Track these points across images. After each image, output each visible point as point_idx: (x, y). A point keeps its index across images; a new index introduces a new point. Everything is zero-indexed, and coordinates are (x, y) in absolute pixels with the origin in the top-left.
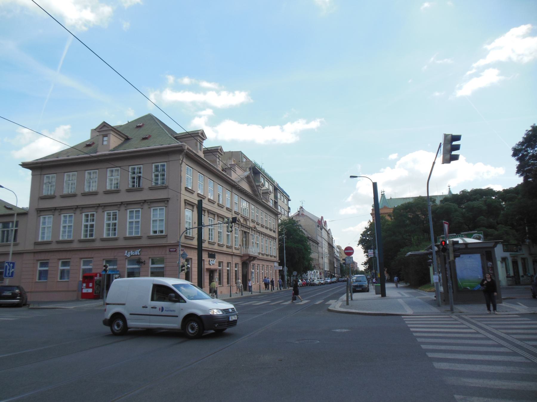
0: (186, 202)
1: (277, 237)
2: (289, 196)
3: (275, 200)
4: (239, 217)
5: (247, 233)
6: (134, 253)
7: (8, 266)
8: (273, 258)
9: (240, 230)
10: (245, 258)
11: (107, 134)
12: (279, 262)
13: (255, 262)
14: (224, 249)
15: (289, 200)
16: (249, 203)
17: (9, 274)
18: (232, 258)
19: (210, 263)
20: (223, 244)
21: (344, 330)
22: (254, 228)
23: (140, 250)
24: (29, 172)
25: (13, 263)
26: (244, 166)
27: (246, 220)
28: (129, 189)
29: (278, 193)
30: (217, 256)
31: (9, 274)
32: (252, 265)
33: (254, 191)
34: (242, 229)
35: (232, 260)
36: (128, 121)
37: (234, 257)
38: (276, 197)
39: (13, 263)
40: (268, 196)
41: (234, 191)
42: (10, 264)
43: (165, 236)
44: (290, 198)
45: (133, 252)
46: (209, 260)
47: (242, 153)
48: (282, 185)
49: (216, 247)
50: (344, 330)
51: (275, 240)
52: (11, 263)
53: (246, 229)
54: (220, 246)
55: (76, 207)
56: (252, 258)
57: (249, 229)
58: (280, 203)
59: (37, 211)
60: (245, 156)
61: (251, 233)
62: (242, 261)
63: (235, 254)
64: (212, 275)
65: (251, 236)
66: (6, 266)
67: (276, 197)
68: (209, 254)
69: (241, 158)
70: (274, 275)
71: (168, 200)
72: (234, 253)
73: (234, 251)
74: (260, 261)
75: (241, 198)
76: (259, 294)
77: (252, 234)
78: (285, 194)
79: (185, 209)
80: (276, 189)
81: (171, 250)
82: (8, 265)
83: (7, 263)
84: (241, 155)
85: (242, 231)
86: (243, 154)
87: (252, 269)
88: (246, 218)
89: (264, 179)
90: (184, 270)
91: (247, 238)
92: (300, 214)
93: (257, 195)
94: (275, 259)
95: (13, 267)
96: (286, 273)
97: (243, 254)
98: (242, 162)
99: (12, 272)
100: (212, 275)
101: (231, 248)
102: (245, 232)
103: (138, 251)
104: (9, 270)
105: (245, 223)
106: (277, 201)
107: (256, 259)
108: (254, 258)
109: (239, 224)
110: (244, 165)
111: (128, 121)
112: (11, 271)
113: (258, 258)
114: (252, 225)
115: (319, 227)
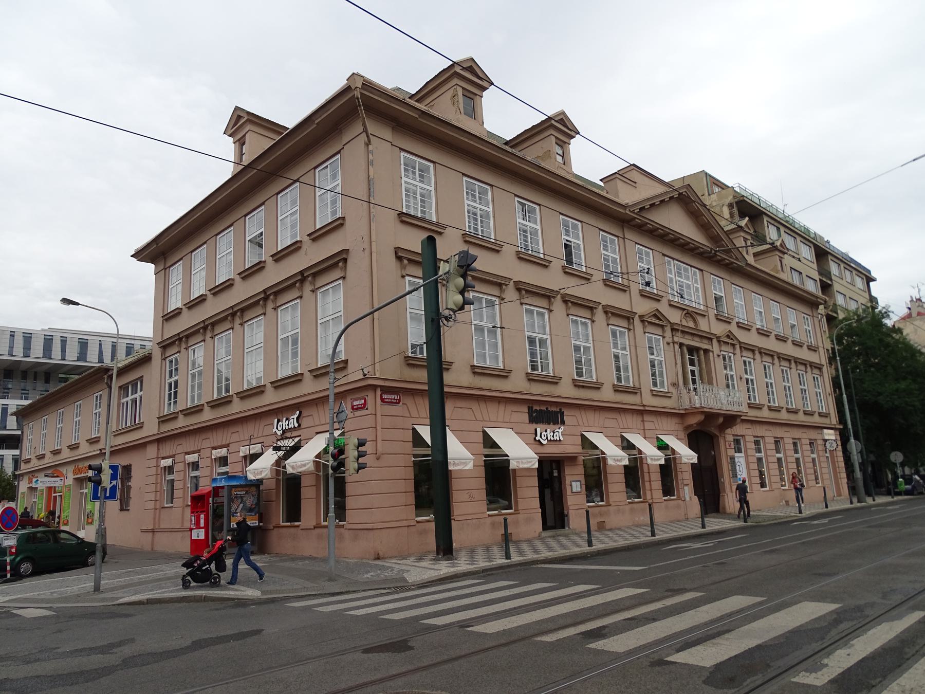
0: (400, 254)
1: (824, 362)
2: (869, 272)
3: (824, 279)
4: (664, 308)
5: (702, 352)
6: (288, 425)
8: (816, 419)
9: (668, 344)
10: (693, 420)
12: (839, 429)
13: (739, 429)
14: (607, 395)
15: (869, 279)
18: (643, 421)
19: (538, 438)
22: (728, 336)
23: (298, 412)
24: (150, 268)
26: (714, 204)
27: (690, 314)
29: (832, 264)
30: (570, 417)
32: (730, 438)
33: (715, 239)
34: (676, 339)
35: (644, 426)
37: (646, 418)
38: (824, 272)
41: (629, 235)
43: (341, 365)
44: (874, 274)
45: (287, 421)
46: (536, 430)
47: (706, 174)
48: (839, 242)
49: (565, 391)
51: (816, 371)
53: (697, 339)
54: (583, 387)
56: (721, 420)
57: (711, 340)
60: (715, 182)
62: (686, 428)
63: (647, 408)
64: (556, 474)
65: (719, 363)
67: (824, 272)
68: (530, 412)
69: (705, 186)
70: (824, 465)
71: (344, 256)
72: (644, 406)
73: (650, 401)
74: (765, 427)
75: (664, 255)
76: (740, 523)
77: (723, 353)
78: (852, 265)
79: (403, 277)
80: (822, 253)
81: (355, 403)
84: (705, 178)
85: (681, 345)
86: (710, 176)
87: (731, 452)
88: (691, 309)
89: (778, 229)
91: (704, 366)
92: (914, 315)
94: (825, 421)
96: (856, 457)
97: (686, 409)
98: (709, 195)
100: (556, 474)
101: (636, 393)
102: (692, 350)
103: (295, 417)
105: (691, 324)
106: (829, 282)
107: (738, 420)
108: (731, 419)
109: (662, 327)
110: (715, 201)
113: (742, 418)
114: (718, 329)
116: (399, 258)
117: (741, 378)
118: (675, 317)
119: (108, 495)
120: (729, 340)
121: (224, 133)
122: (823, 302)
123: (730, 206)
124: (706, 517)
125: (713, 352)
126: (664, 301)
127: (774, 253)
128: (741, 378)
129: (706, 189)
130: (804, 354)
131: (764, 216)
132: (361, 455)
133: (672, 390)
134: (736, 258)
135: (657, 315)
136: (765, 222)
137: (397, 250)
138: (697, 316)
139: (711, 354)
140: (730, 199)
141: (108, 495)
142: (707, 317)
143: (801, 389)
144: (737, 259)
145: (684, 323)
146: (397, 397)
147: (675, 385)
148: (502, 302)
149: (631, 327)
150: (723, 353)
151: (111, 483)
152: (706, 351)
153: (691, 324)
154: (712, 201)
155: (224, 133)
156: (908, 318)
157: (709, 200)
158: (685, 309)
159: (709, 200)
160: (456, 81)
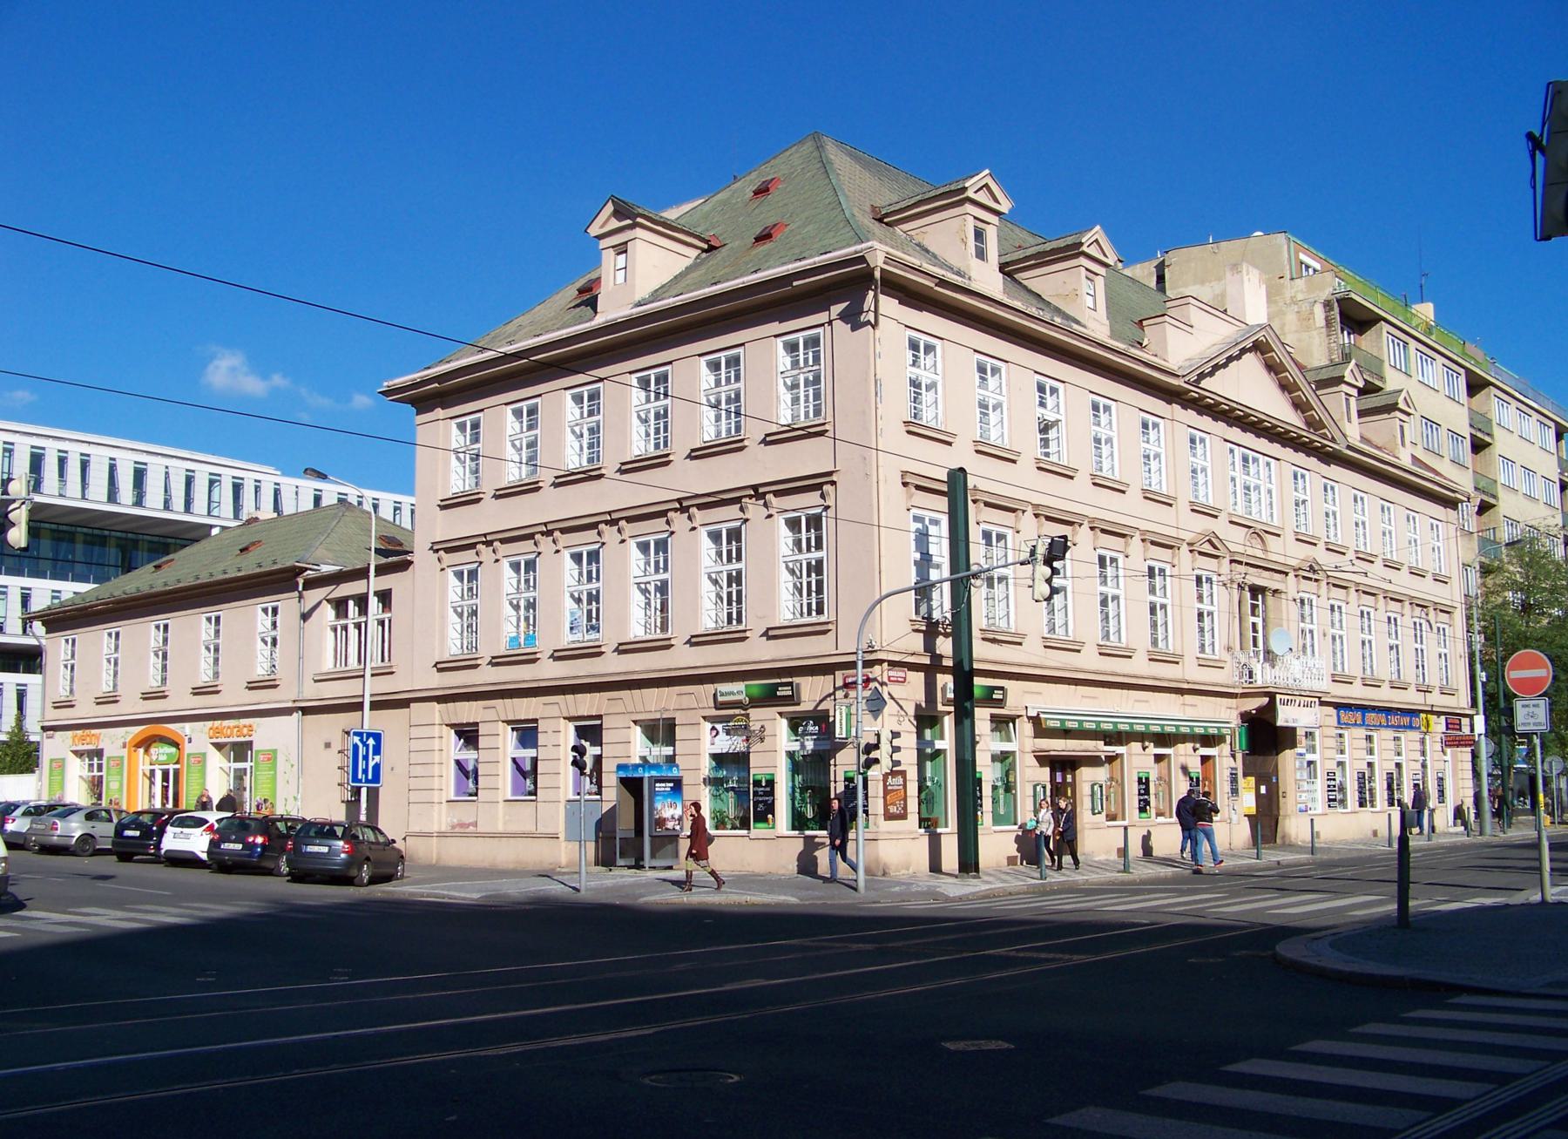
3: (1479, 435)
4: (1221, 527)
11: (626, 243)
17: (365, 771)
20: (1126, 649)
21: (993, 1045)
25: (377, 737)
27: (1260, 534)
28: (703, 445)
31: (365, 771)
39: (377, 737)
40: (1398, 422)
42: (367, 739)
50: (993, 1045)
52: (369, 735)
58: (1502, 443)
61: (1292, 593)
65: (1294, 609)
77: (1301, 594)
82: (361, 741)
83: (355, 734)
84: (1286, 247)
88: (1259, 526)
90: (877, 761)
93: (1314, 424)
95: (377, 751)
98: (1292, 279)
99: (377, 768)
102: (1256, 591)
104: (366, 758)
112: (371, 764)
114: (1296, 554)
116: (905, 484)
117: (1325, 635)
118: (1236, 539)
119: (370, 777)
120: (1311, 572)
123: (1327, 305)
124: (1264, 848)
126: (1223, 517)
127: (1393, 414)
128: (1325, 635)
129: (1288, 267)
130: (1426, 589)
131: (1383, 322)
132: (896, 749)
133: (1226, 656)
134: (1333, 437)
136: (1385, 334)
137: (904, 473)
143: (1417, 649)
144: (1333, 440)
145: (1250, 551)
146: (903, 675)
147: (1229, 649)
148: (1062, 575)
149: (1176, 562)
150: (1301, 594)
153: (1260, 554)
158: (1250, 527)
159: (1292, 288)
160: (969, 208)
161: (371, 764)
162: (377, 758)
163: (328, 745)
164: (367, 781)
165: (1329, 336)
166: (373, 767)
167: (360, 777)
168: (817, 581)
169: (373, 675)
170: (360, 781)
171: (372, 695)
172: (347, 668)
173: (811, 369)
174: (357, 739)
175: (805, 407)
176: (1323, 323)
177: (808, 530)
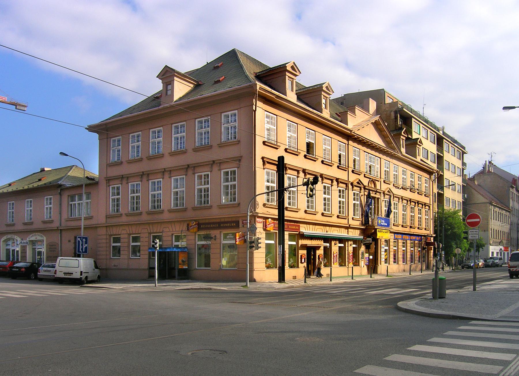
3: (439, 153)
4: (361, 178)
7: (80, 240)
11: (171, 81)
16: (380, 158)
17: (82, 249)
25: (86, 239)
31: (82, 249)
36: (207, 62)
39: (86, 239)
42: (83, 239)
52: (83, 238)
55: (142, 174)
59: (106, 180)
66: (79, 241)
82: (81, 239)
83: (79, 237)
95: (86, 243)
104: (82, 245)
106: (442, 155)
110: (388, 108)
111: (207, 62)
112: (84, 247)
115: (514, 189)
119: (84, 251)
121: (157, 77)
122: (436, 172)
125: (381, 199)
135: (359, 183)
138: (376, 181)
139: (380, 200)
140: (396, 108)
141: (84, 251)
142: (380, 182)
151: (85, 245)
152: (378, 199)
154: (386, 108)
155: (157, 77)
156: (482, 173)
157: (384, 106)
158: (370, 178)
159: (384, 106)
161: (84, 247)
162: (86, 245)
163: (69, 241)
164: (83, 252)
165: (395, 122)
166: (85, 248)
167: (80, 251)
168: (155, 198)
169: (84, 219)
170: (81, 252)
171: (84, 226)
172: (76, 217)
173: (233, 123)
174: (79, 239)
175: (231, 136)
176: (394, 117)
177: (231, 175)
